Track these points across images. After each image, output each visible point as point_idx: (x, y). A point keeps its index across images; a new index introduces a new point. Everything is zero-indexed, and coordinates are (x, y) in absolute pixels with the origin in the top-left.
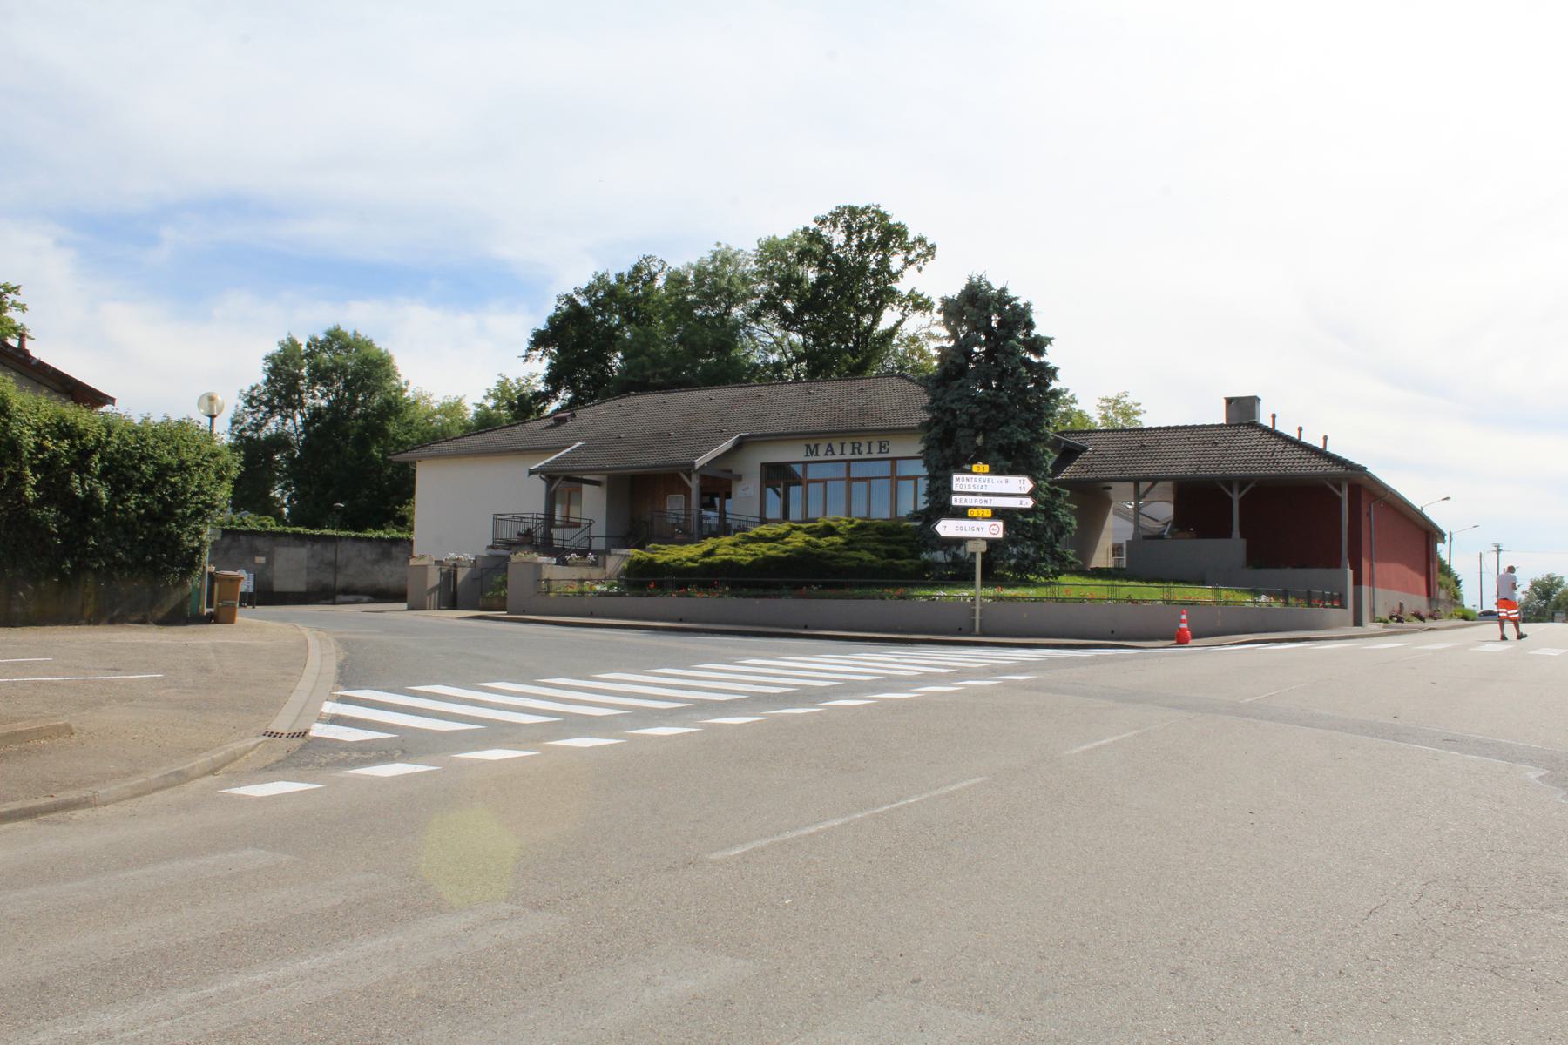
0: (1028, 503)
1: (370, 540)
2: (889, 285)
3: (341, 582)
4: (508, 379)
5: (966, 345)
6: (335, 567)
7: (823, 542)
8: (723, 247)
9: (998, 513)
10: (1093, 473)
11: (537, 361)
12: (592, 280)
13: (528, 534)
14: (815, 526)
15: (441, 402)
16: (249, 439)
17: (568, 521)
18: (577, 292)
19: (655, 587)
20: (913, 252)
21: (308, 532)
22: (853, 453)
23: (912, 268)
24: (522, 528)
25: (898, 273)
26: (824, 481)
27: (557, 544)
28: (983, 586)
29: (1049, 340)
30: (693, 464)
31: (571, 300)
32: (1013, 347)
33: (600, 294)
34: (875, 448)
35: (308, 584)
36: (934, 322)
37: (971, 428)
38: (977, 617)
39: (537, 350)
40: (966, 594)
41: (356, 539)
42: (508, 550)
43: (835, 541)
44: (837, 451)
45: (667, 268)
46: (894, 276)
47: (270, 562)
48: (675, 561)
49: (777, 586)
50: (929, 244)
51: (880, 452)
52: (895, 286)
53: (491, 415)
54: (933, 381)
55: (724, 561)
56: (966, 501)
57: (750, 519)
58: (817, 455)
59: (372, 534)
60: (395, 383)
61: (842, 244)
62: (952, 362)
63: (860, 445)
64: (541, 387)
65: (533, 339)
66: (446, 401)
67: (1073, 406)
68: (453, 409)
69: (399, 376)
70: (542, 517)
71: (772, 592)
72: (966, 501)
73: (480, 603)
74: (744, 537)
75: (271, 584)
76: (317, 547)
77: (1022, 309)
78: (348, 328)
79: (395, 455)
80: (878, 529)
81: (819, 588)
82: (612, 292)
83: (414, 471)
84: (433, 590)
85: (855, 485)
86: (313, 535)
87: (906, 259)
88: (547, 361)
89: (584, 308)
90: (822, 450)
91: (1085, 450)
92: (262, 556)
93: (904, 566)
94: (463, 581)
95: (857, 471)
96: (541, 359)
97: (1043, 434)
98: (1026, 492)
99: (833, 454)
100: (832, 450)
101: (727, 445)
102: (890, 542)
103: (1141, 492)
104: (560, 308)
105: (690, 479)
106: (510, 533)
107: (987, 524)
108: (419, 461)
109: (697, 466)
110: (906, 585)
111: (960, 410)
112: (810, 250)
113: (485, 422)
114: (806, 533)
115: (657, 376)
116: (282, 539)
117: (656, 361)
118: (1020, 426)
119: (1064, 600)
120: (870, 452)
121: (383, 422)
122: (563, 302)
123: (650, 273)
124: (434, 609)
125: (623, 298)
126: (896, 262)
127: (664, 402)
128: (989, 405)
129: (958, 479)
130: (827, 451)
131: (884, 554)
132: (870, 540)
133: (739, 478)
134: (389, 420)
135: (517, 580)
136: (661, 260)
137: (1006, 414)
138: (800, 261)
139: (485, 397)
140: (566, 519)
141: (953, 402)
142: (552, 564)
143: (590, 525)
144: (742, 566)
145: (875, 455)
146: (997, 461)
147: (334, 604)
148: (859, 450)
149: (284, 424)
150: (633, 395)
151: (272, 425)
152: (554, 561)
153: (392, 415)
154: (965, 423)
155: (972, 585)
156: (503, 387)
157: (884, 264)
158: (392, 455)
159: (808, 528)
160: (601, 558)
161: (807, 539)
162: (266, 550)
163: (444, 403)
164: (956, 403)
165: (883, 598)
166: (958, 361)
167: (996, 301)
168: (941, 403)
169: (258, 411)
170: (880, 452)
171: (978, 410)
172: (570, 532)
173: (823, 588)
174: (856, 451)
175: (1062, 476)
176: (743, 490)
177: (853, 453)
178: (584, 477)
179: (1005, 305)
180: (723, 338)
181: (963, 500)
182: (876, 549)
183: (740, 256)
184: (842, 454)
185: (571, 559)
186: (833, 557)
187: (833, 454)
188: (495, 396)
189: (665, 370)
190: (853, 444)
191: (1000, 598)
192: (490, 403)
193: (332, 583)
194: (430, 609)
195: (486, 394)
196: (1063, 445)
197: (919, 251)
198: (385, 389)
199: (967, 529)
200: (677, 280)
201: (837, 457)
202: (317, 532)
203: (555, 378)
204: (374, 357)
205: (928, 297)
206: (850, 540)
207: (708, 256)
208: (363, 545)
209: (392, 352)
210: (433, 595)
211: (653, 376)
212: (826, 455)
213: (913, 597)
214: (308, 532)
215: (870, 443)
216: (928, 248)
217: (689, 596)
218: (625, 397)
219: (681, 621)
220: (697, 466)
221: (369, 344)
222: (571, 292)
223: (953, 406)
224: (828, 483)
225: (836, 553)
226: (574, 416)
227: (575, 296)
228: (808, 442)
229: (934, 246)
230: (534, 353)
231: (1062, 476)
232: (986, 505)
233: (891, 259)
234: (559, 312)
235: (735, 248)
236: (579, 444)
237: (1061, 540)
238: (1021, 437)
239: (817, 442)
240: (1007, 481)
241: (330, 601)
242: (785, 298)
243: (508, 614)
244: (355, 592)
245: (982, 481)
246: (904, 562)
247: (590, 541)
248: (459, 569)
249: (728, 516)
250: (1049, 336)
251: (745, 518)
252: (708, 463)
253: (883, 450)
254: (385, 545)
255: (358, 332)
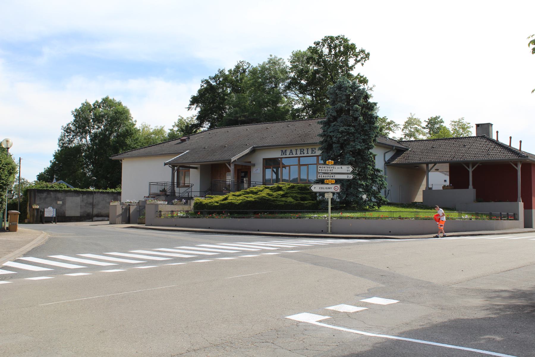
0: (351, 177)
1: (108, 193)
2: (348, 72)
3: (95, 212)
4: (183, 118)
5: (337, 108)
6: (93, 205)
7: (275, 194)
8: (273, 57)
9: (337, 181)
10: (408, 160)
11: (194, 110)
12: (217, 73)
13: (164, 191)
14: (274, 187)
15: (154, 129)
16: (66, 147)
17: (184, 185)
18: (210, 78)
19: (200, 213)
20: (359, 56)
21: (81, 190)
22: (301, 154)
23: (359, 64)
24: (161, 188)
25: (353, 66)
26: (289, 166)
27: (177, 195)
28: (332, 213)
29: (377, 103)
30: (231, 160)
31: (207, 82)
32: (357, 108)
33: (221, 79)
34: (310, 151)
35: (81, 213)
36: (369, 89)
37: (338, 144)
38: (329, 226)
39: (193, 105)
40: (326, 216)
41: (102, 193)
42: (153, 198)
43: (280, 193)
44: (294, 153)
45: (250, 66)
46: (351, 68)
47: (64, 204)
48: (210, 203)
49: (247, 213)
50: (366, 53)
51: (312, 153)
52: (351, 72)
53: (175, 134)
54: (324, 123)
55: (229, 203)
56: (324, 176)
57: (257, 183)
58: (286, 155)
59: (109, 190)
60: (130, 121)
61: (327, 54)
62: (331, 115)
63: (304, 150)
64: (196, 122)
65: (191, 100)
66: (156, 128)
67: (442, 124)
68: (159, 132)
69: (132, 118)
70: (171, 183)
71: (247, 216)
72: (324, 176)
73: (138, 221)
74: (245, 192)
75: (65, 213)
76: (85, 196)
77: (361, 91)
78: (111, 98)
79: (113, 157)
80: (299, 188)
81: (267, 214)
82: (226, 78)
83: (121, 163)
84: (119, 215)
85: (302, 167)
86: (83, 191)
87: (356, 60)
88: (199, 109)
89: (214, 85)
90: (288, 153)
91: (407, 150)
92: (61, 201)
93: (306, 204)
94: (132, 212)
95: (303, 161)
96: (195, 109)
97: (371, 145)
98: (350, 172)
99: (292, 154)
100: (292, 153)
101: (247, 151)
102: (303, 193)
103: (429, 169)
104: (203, 86)
105: (230, 167)
106: (156, 190)
107: (333, 186)
108: (123, 159)
109: (232, 161)
110: (300, 212)
111: (333, 136)
112: (312, 58)
113: (172, 137)
114: (270, 190)
115: (242, 116)
116: (69, 193)
117: (244, 109)
118: (360, 142)
119: (369, 218)
120: (308, 153)
121: (124, 139)
122: (204, 83)
123: (243, 69)
124: (120, 224)
125: (230, 81)
126: (351, 62)
127: (228, 132)
128: (346, 134)
129: (320, 167)
130: (290, 153)
131: (299, 199)
132: (294, 193)
133: (254, 165)
134: (127, 138)
135: (149, 213)
136: (248, 63)
137: (354, 137)
138: (308, 63)
139: (174, 126)
140: (173, 183)
141: (331, 132)
142: (165, 204)
143: (192, 186)
144: (236, 204)
145: (310, 154)
146: (349, 158)
147: (92, 221)
148: (303, 152)
149: (81, 141)
150: (216, 128)
151: (76, 141)
152: (167, 203)
153: (128, 136)
154: (336, 142)
155: (327, 212)
156: (181, 121)
157: (346, 62)
158: (112, 157)
159: (271, 188)
160: (189, 201)
161: (268, 192)
162: (62, 198)
163: (155, 129)
164: (332, 133)
165: (291, 218)
166: (333, 115)
167: (350, 88)
168: (326, 133)
169: (70, 135)
170: (312, 153)
171: (341, 136)
172: (182, 190)
173: (269, 214)
174: (302, 153)
175: (394, 162)
176: (256, 170)
177: (301, 154)
178: (191, 166)
179: (355, 89)
180: (272, 99)
181: (323, 176)
182: (296, 197)
183: (281, 61)
184: (296, 154)
185: (175, 202)
186: (274, 201)
187: (292, 154)
188: (177, 126)
189: (245, 114)
190: (301, 150)
191: (341, 218)
192: (176, 129)
193: (92, 212)
194: (118, 224)
195: (174, 125)
196: (394, 148)
197: (362, 56)
198: (125, 124)
199: (324, 188)
200: (254, 72)
201: (294, 155)
202: (85, 190)
203: (202, 118)
204: (120, 110)
205: (365, 77)
206: (287, 193)
207: (266, 61)
208: (105, 195)
209: (128, 107)
210: (119, 217)
211: (240, 117)
212: (290, 154)
213: (305, 217)
214: (81, 190)
215: (308, 149)
216: (366, 55)
217: (213, 218)
218: (213, 129)
219: (209, 228)
220: (232, 161)
221: (120, 104)
222: (208, 78)
223: (330, 134)
224: (291, 166)
225: (275, 199)
226: (189, 138)
227: (209, 80)
228: (282, 149)
229: (369, 54)
230: (192, 106)
231: (394, 162)
232: (332, 178)
233: (349, 60)
234: (203, 87)
235: (279, 57)
236: (187, 151)
237: (381, 191)
238: (359, 147)
239: (286, 149)
240: (341, 168)
241: (91, 220)
242: (301, 79)
243: (146, 226)
244: (102, 216)
245: (331, 168)
246: (306, 202)
247: (188, 193)
248: (131, 207)
249: (251, 182)
250: (375, 102)
251: (255, 183)
252: (238, 159)
253: (313, 152)
254: (115, 195)
255: (115, 99)
